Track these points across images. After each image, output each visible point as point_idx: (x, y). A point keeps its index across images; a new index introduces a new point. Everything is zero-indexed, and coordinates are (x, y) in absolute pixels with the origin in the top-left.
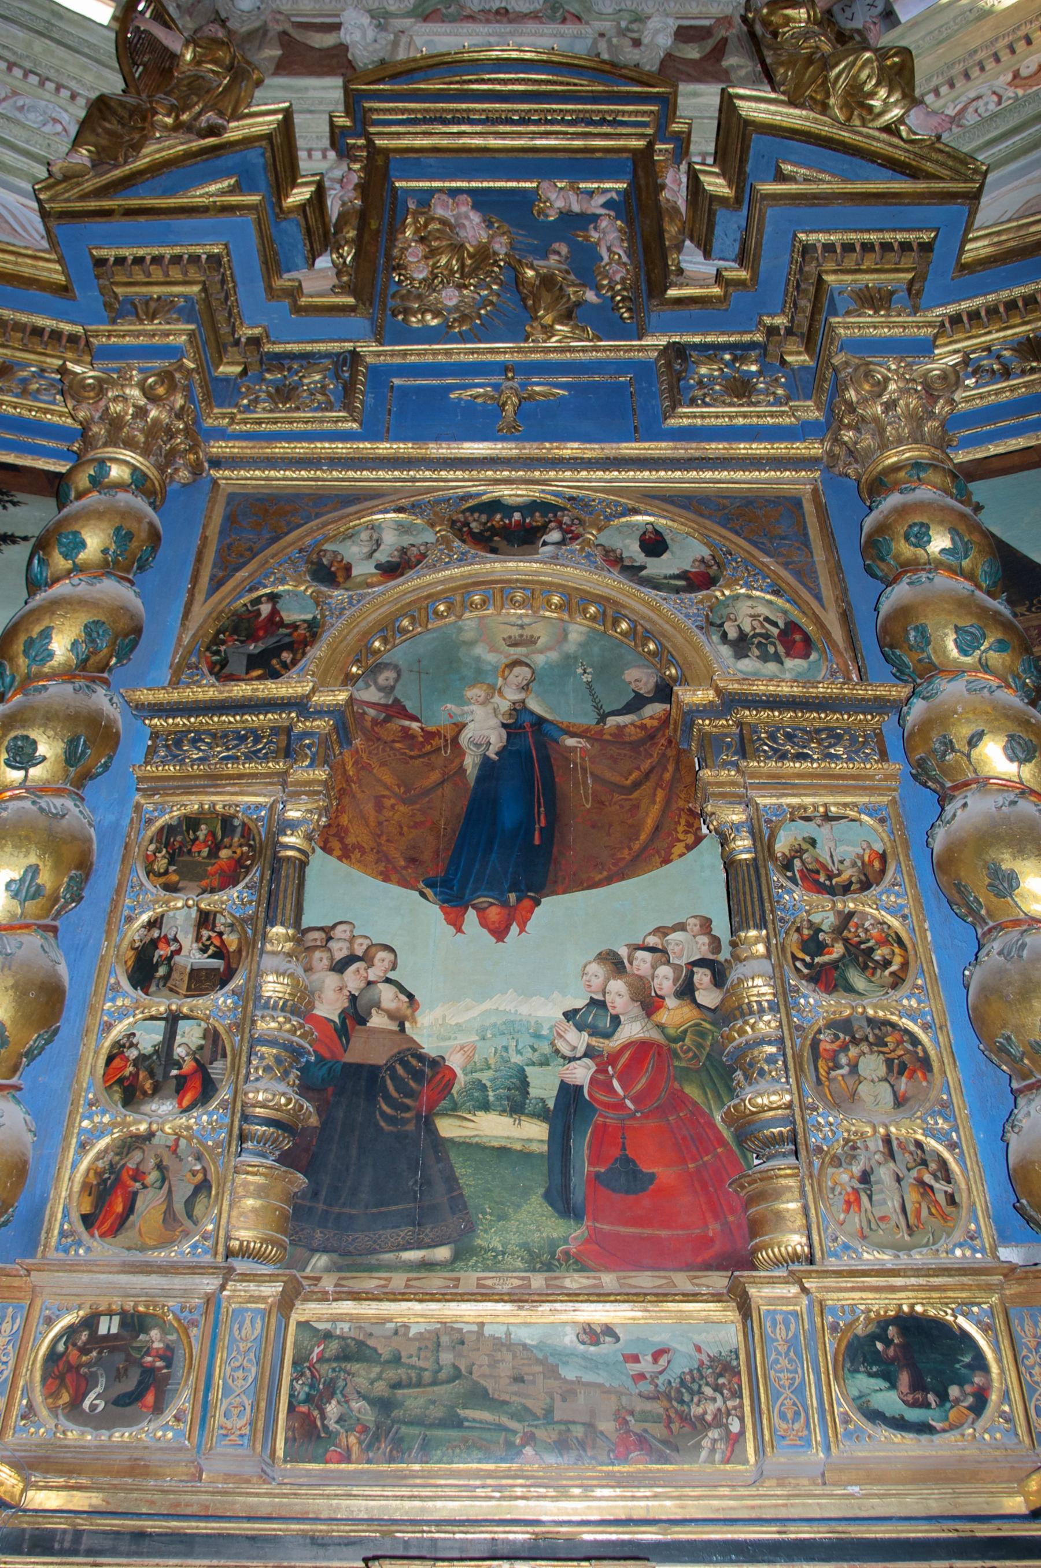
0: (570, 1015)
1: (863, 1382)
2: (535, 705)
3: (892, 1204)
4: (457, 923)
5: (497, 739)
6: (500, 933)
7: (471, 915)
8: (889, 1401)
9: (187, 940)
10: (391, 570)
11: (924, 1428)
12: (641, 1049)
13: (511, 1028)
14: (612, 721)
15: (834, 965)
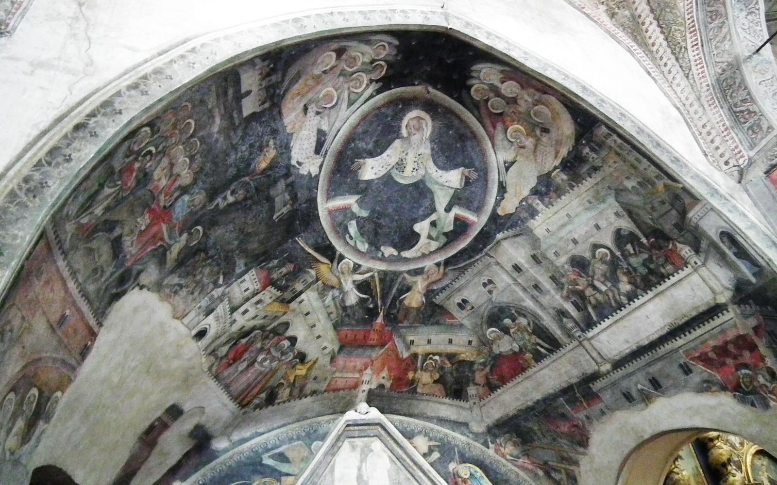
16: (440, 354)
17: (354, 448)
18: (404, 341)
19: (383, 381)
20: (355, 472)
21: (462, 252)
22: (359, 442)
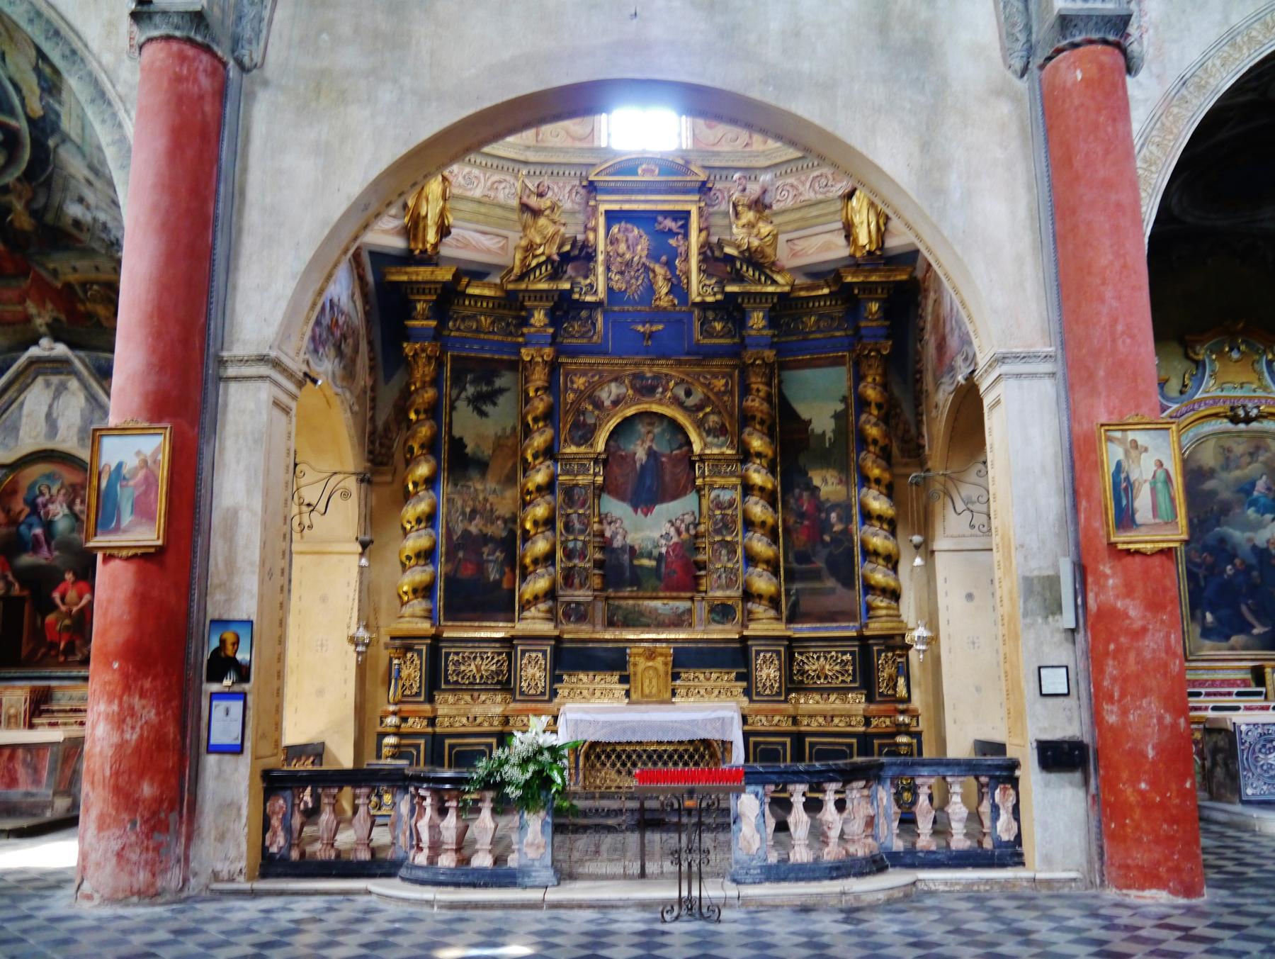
1: (713, 615)
2: (655, 447)
3: (724, 581)
4: (636, 511)
5: (644, 458)
7: (639, 511)
8: (717, 618)
9: (576, 522)
11: (723, 623)
12: (676, 544)
13: (649, 539)
15: (720, 528)
16: (97, 283)
17: (48, 384)
18: (46, 269)
19: (55, 314)
20: (45, 409)
21: (31, 163)
22: (55, 380)
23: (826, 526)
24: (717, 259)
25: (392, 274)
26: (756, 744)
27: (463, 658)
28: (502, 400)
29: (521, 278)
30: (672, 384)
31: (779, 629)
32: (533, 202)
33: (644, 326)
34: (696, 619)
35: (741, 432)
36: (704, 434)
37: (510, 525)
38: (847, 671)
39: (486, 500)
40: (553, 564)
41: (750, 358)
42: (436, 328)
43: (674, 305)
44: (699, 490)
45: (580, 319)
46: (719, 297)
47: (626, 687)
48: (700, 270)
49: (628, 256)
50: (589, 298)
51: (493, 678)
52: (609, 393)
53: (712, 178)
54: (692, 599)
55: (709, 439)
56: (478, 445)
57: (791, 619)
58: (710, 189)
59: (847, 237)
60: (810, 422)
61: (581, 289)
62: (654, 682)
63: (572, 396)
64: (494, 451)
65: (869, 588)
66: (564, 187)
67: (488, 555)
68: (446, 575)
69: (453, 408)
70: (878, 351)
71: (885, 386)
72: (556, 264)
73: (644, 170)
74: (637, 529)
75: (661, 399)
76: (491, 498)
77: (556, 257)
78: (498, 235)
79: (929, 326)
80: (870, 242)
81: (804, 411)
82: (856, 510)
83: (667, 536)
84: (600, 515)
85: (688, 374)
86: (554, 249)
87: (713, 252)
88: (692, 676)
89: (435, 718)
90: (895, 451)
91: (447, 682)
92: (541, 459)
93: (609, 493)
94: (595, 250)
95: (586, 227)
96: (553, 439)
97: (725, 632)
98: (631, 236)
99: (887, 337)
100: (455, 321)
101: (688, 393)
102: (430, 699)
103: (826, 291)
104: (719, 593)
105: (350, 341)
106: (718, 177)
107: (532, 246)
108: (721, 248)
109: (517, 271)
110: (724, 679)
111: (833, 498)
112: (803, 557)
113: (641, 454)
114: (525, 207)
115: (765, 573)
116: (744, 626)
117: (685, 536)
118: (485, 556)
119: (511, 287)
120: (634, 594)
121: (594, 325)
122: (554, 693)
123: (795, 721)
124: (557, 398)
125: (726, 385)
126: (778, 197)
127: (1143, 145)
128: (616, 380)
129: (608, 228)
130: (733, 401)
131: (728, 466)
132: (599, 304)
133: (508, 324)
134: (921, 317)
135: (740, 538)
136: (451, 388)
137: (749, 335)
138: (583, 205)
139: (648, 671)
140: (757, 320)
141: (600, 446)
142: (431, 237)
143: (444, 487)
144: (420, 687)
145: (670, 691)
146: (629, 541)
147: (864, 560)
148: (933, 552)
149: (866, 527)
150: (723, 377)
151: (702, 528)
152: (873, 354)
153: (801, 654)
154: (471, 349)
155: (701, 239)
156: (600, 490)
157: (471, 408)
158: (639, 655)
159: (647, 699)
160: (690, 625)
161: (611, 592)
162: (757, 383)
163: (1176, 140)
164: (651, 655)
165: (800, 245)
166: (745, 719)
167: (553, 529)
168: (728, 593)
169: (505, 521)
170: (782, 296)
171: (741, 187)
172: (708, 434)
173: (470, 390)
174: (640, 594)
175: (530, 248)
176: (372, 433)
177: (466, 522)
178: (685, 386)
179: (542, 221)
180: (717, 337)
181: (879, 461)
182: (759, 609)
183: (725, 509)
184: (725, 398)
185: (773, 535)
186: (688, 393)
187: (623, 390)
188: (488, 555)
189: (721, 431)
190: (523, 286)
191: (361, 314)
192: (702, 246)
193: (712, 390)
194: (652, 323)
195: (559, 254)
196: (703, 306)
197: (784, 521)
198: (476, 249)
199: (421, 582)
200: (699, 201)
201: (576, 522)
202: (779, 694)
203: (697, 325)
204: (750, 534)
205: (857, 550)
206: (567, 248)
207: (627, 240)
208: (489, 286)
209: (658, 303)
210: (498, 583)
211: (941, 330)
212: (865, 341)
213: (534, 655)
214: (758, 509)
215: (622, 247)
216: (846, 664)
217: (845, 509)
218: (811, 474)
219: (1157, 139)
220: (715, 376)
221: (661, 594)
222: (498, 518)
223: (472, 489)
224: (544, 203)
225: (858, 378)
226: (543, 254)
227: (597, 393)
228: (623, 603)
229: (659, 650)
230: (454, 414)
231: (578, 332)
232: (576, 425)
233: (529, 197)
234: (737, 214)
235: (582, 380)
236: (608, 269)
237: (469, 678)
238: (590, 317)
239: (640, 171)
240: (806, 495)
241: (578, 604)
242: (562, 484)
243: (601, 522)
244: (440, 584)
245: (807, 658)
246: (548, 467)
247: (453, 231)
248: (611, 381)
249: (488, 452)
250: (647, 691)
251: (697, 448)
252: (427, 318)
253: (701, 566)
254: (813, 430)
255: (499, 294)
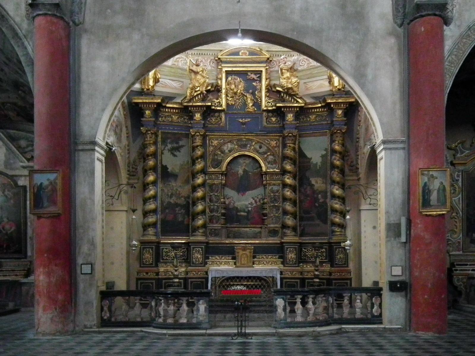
0: (249, 204)
4: (238, 194)
5: (242, 173)
6: (243, 195)
9: (214, 198)
10: (230, 151)
12: (255, 206)
14: (255, 171)
23: (316, 200)
24: (274, 91)
25: (135, 99)
26: (286, 282)
27: (169, 250)
28: (183, 150)
29: (190, 101)
30: (254, 143)
31: (296, 239)
32: (194, 68)
33: (242, 120)
34: (263, 235)
35: (282, 163)
36: (267, 163)
37: (187, 200)
38: (323, 255)
39: (177, 190)
40: (205, 215)
41: (286, 133)
42: (154, 121)
43: (255, 111)
44: (265, 186)
45: (215, 117)
46: (274, 108)
47: (234, 261)
48: (266, 96)
49: (235, 90)
50: (218, 108)
51: (181, 258)
52: (227, 147)
53: (272, 56)
54: (261, 228)
55: (269, 165)
56: (173, 168)
57: (301, 235)
58: (271, 61)
59: (330, 82)
60: (311, 158)
61: (215, 104)
62: (246, 259)
63: (212, 148)
64: (180, 171)
65: (333, 224)
66: (207, 60)
67: (179, 211)
68: (161, 219)
69: (162, 153)
70: (341, 130)
71: (343, 145)
72: (204, 95)
73: (242, 53)
74: (239, 201)
75: (249, 149)
76: (179, 189)
77: (205, 92)
78: (179, 81)
79: (362, 121)
80: (339, 85)
81: (308, 154)
82: (329, 194)
83: (251, 204)
84: (224, 195)
85: (260, 139)
86: (204, 89)
87: (271, 88)
88: (261, 257)
89: (159, 272)
90: (347, 170)
91: (163, 259)
92: (199, 174)
93: (227, 187)
94: (221, 88)
95: (217, 77)
96: (204, 166)
97: (275, 240)
98: (236, 81)
99: (345, 125)
100: (162, 117)
101: (260, 147)
102: (157, 266)
103: (320, 105)
104: (272, 226)
105: (119, 127)
106: (274, 55)
107: (194, 87)
108: (275, 88)
109: (188, 98)
110: (275, 258)
111: (320, 189)
112: (307, 212)
113: (241, 172)
114: (191, 71)
115: (291, 218)
116: (282, 238)
117: (258, 203)
118: (177, 212)
119: (185, 104)
120: (238, 226)
121: (221, 119)
122: (206, 263)
123: (301, 273)
124: (206, 150)
125: (276, 143)
126: (301, 64)
127: (449, 56)
128: (230, 142)
129: (227, 78)
130: (279, 150)
131: (277, 176)
132: (223, 111)
133: (184, 119)
134: (360, 116)
135: (281, 205)
136: (161, 145)
137: (287, 124)
138: (216, 68)
139: (243, 255)
140: (290, 117)
141: (224, 169)
142: (151, 83)
143: (160, 185)
144: (152, 261)
145: (252, 263)
146: (236, 205)
147: (331, 213)
148: (360, 210)
149: (333, 201)
150: (275, 141)
151: (266, 200)
152: (338, 131)
153: (305, 249)
154: (169, 129)
155: (267, 83)
156: (224, 185)
157: (170, 153)
158: (240, 249)
159: (243, 266)
160: (260, 238)
161: (228, 225)
162: (290, 144)
163: (463, 53)
164: (244, 249)
165: (310, 84)
166: (281, 273)
167: (205, 201)
168: (276, 225)
169: (185, 198)
170: (301, 108)
171: (284, 62)
172: (269, 164)
173: (169, 146)
174: (240, 226)
175: (193, 88)
176: (129, 163)
177: (169, 199)
178: (259, 144)
179: (199, 77)
180: (273, 124)
181: (339, 174)
182: (288, 232)
183: (275, 193)
184: (276, 149)
185: (294, 203)
186: (260, 147)
187: (233, 146)
188: (179, 211)
189: (275, 162)
190: (191, 104)
191: (123, 116)
192: (267, 86)
193: (271, 145)
194: (245, 118)
195: (206, 91)
196: (268, 111)
197: (299, 198)
198: (170, 87)
199: (152, 222)
200: (266, 66)
201: (214, 198)
202: (295, 264)
203: (265, 119)
204: (285, 203)
205: (329, 209)
206: (209, 88)
207: (235, 83)
208: (176, 103)
209: (248, 110)
210: (183, 221)
211: (367, 123)
212: (335, 126)
213: (198, 249)
214: (288, 193)
215: (233, 87)
216: (323, 253)
217: (324, 193)
218: (311, 179)
219: (455, 53)
220: (272, 140)
221: (249, 226)
222: (182, 197)
223: (171, 186)
224: (199, 69)
225: (332, 141)
226: (199, 90)
227: (222, 147)
228: (233, 229)
229: (248, 247)
230: (163, 156)
231: (214, 122)
232: (213, 160)
233: (192, 66)
234: (282, 73)
235: (216, 142)
236: (227, 96)
237: (171, 258)
238: (219, 116)
239: (240, 54)
240: (309, 187)
241: (215, 230)
242: (208, 183)
243: (224, 198)
244: (159, 223)
245: (307, 250)
246: (202, 177)
247: (160, 80)
248: (228, 142)
249: (177, 171)
250: (243, 262)
251: (264, 169)
252: (151, 117)
253: (265, 215)
254: (312, 162)
255: (180, 107)
